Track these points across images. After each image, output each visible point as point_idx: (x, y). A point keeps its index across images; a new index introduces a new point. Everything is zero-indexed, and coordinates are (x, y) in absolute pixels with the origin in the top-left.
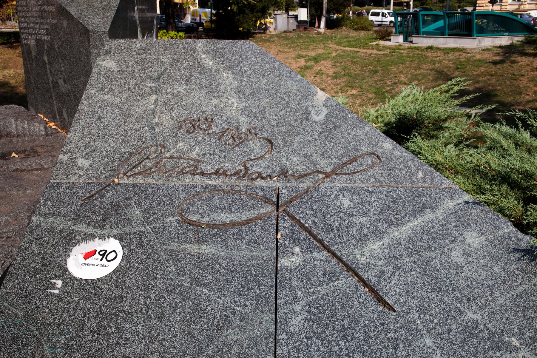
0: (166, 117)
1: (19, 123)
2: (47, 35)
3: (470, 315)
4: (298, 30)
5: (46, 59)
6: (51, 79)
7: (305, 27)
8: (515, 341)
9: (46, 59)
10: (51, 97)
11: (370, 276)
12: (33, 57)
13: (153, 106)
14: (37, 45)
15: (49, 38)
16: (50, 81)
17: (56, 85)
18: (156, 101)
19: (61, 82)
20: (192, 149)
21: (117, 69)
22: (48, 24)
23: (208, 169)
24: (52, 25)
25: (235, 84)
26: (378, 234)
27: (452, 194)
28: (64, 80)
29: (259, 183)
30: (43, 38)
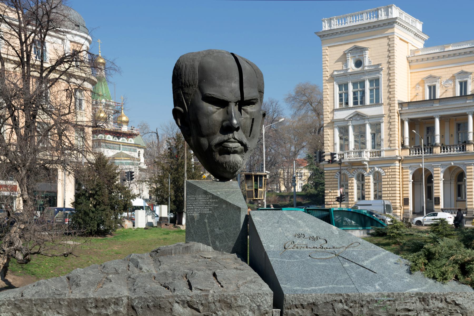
0: (288, 234)
1: (203, 246)
2: (209, 211)
3: (395, 273)
4: (159, 226)
5: (206, 221)
6: (208, 229)
7: (166, 223)
8: (406, 277)
9: (206, 221)
10: (207, 237)
11: (368, 267)
12: (195, 221)
13: (282, 231)
14: (200, 216)
15: (211, 212)
16: (208, 230)
17: (212, 231)
18: (282, 229)
19: (217, 230)
20: (302, 242)
21: (261, 220)
22: (211, 207)
23: (311, 247)
24: (214, 207)
25: (305, 224)
26: (367, 260)
27: (383, 251)
28: (220, 229)
29: (327, 250)
30: (206, 212)
